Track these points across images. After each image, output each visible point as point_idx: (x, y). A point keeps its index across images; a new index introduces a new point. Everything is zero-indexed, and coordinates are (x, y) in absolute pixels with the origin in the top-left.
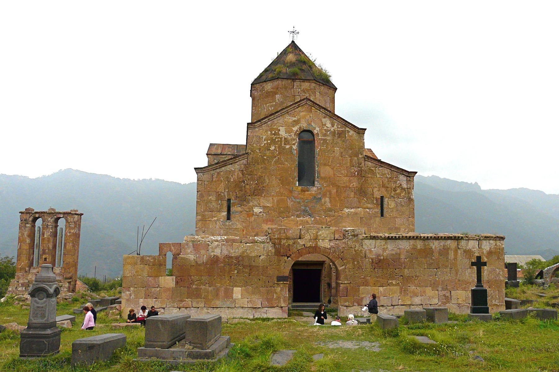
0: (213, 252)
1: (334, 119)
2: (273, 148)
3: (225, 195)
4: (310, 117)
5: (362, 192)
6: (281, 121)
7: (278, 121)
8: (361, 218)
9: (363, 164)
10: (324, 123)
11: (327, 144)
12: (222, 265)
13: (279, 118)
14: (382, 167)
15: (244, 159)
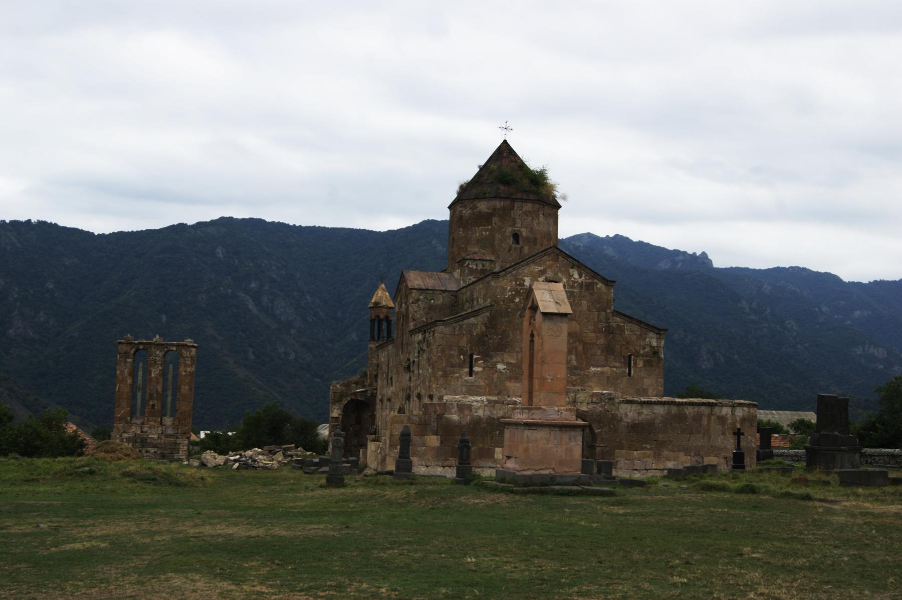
0: (476, 412)
1: (583, 270)
2: (517, 300)
3: (467, 350)
4: (557, 266)
5: (609, 350)
6: (526, 271)
7: (523, 271)
8: (608, 378)
9: (611, 320)
10: (571, 274)
11: (575, 297)
12: (485, 425)
13: (523, 268)
14: (631, 323)
15: (487, 312)
